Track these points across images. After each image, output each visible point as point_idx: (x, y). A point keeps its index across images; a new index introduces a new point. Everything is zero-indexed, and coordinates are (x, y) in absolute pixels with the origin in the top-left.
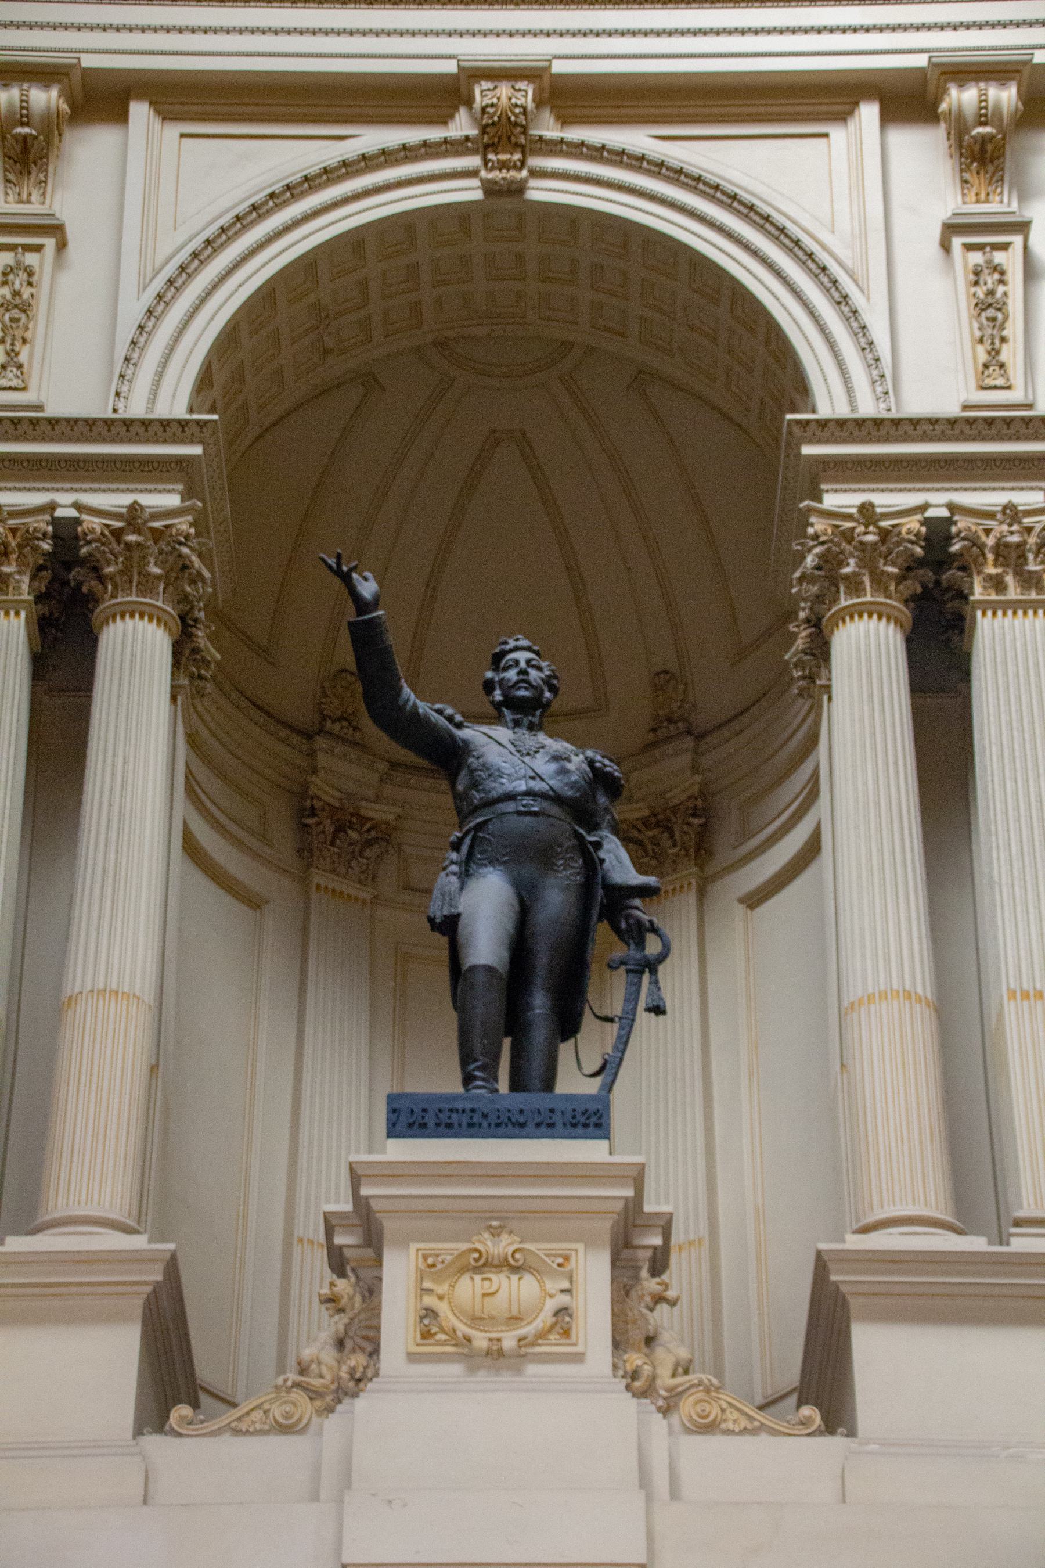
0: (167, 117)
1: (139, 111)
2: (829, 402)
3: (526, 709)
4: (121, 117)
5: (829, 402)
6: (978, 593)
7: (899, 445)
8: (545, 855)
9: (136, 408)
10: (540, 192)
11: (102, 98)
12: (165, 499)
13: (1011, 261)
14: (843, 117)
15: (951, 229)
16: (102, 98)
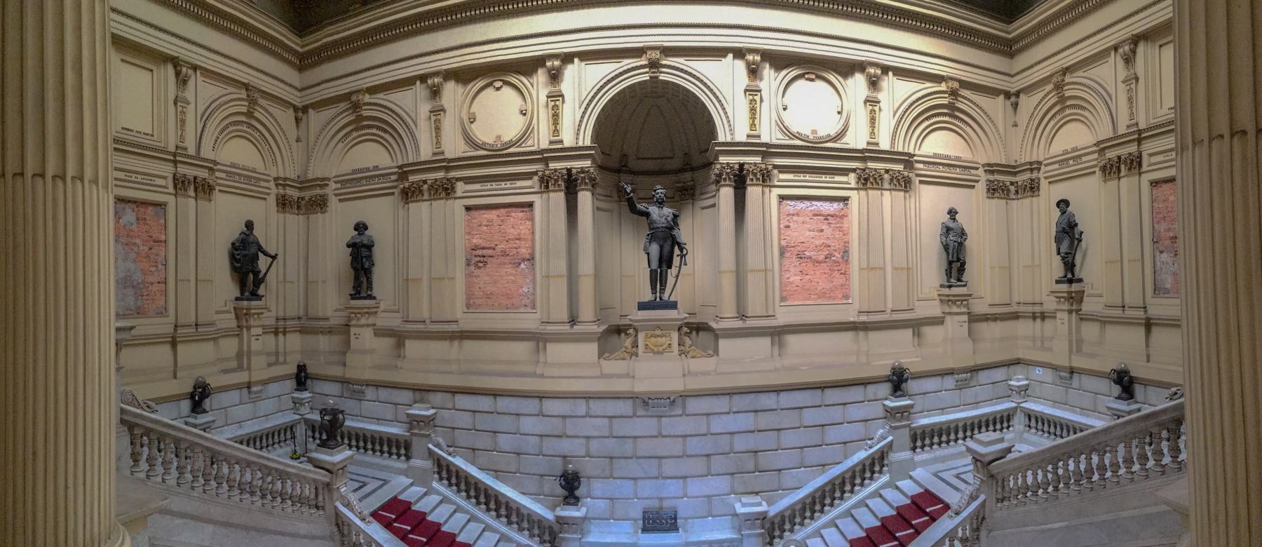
0: (582, 60)
1: (576, 60)
2: (721, 138)
3: (660, 203)
4: (572, 62)
5: (721, 138)
6: (748, 182)
7: (734, 148)
8: (665, 240)
9: (581, 144)
10: (662, 77)
11: (568, 58)
12: (587, 163)
13: (757, 98)
14: (725, 56)
15: (746, 91)
16: (568, 58)
